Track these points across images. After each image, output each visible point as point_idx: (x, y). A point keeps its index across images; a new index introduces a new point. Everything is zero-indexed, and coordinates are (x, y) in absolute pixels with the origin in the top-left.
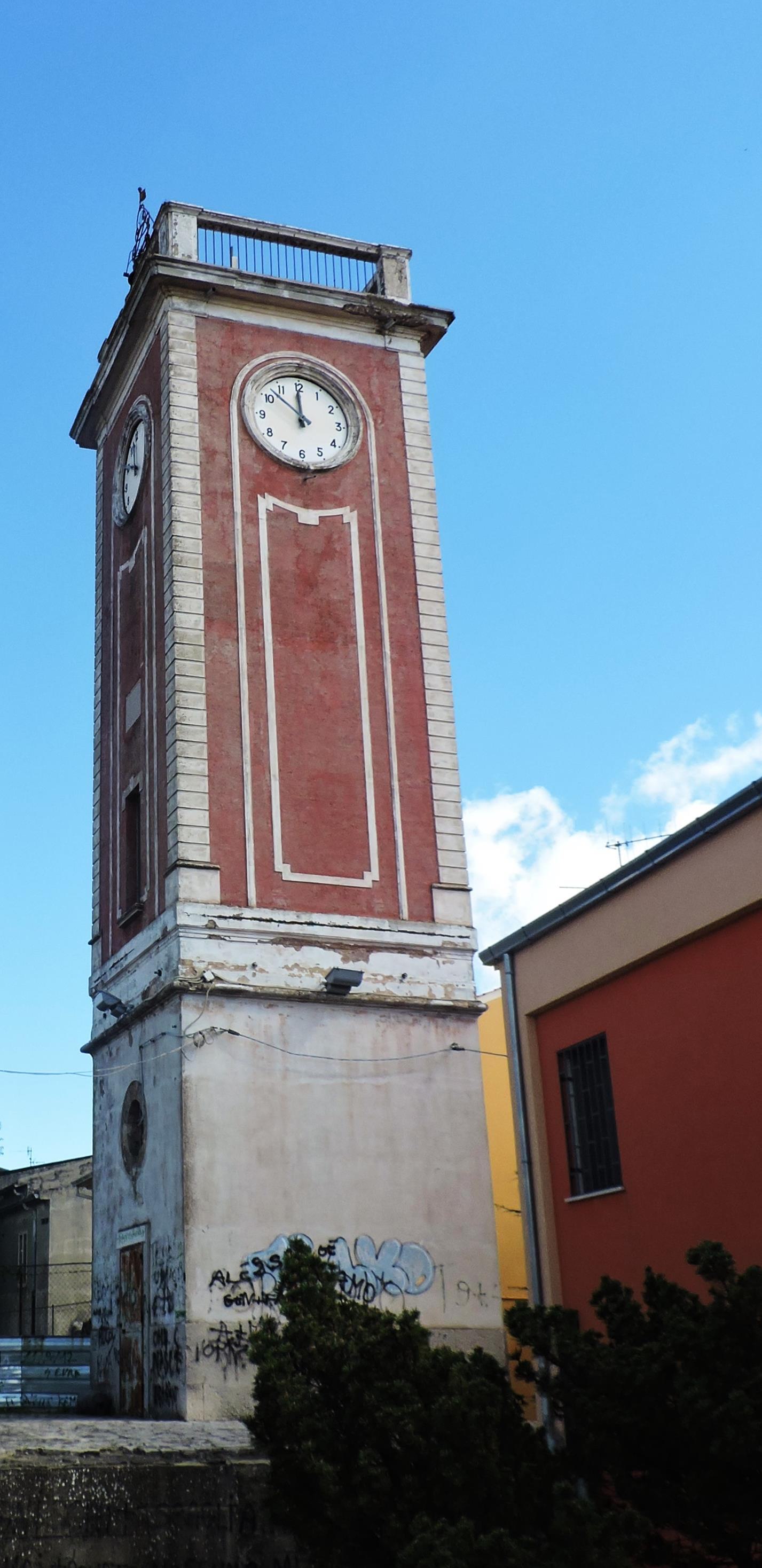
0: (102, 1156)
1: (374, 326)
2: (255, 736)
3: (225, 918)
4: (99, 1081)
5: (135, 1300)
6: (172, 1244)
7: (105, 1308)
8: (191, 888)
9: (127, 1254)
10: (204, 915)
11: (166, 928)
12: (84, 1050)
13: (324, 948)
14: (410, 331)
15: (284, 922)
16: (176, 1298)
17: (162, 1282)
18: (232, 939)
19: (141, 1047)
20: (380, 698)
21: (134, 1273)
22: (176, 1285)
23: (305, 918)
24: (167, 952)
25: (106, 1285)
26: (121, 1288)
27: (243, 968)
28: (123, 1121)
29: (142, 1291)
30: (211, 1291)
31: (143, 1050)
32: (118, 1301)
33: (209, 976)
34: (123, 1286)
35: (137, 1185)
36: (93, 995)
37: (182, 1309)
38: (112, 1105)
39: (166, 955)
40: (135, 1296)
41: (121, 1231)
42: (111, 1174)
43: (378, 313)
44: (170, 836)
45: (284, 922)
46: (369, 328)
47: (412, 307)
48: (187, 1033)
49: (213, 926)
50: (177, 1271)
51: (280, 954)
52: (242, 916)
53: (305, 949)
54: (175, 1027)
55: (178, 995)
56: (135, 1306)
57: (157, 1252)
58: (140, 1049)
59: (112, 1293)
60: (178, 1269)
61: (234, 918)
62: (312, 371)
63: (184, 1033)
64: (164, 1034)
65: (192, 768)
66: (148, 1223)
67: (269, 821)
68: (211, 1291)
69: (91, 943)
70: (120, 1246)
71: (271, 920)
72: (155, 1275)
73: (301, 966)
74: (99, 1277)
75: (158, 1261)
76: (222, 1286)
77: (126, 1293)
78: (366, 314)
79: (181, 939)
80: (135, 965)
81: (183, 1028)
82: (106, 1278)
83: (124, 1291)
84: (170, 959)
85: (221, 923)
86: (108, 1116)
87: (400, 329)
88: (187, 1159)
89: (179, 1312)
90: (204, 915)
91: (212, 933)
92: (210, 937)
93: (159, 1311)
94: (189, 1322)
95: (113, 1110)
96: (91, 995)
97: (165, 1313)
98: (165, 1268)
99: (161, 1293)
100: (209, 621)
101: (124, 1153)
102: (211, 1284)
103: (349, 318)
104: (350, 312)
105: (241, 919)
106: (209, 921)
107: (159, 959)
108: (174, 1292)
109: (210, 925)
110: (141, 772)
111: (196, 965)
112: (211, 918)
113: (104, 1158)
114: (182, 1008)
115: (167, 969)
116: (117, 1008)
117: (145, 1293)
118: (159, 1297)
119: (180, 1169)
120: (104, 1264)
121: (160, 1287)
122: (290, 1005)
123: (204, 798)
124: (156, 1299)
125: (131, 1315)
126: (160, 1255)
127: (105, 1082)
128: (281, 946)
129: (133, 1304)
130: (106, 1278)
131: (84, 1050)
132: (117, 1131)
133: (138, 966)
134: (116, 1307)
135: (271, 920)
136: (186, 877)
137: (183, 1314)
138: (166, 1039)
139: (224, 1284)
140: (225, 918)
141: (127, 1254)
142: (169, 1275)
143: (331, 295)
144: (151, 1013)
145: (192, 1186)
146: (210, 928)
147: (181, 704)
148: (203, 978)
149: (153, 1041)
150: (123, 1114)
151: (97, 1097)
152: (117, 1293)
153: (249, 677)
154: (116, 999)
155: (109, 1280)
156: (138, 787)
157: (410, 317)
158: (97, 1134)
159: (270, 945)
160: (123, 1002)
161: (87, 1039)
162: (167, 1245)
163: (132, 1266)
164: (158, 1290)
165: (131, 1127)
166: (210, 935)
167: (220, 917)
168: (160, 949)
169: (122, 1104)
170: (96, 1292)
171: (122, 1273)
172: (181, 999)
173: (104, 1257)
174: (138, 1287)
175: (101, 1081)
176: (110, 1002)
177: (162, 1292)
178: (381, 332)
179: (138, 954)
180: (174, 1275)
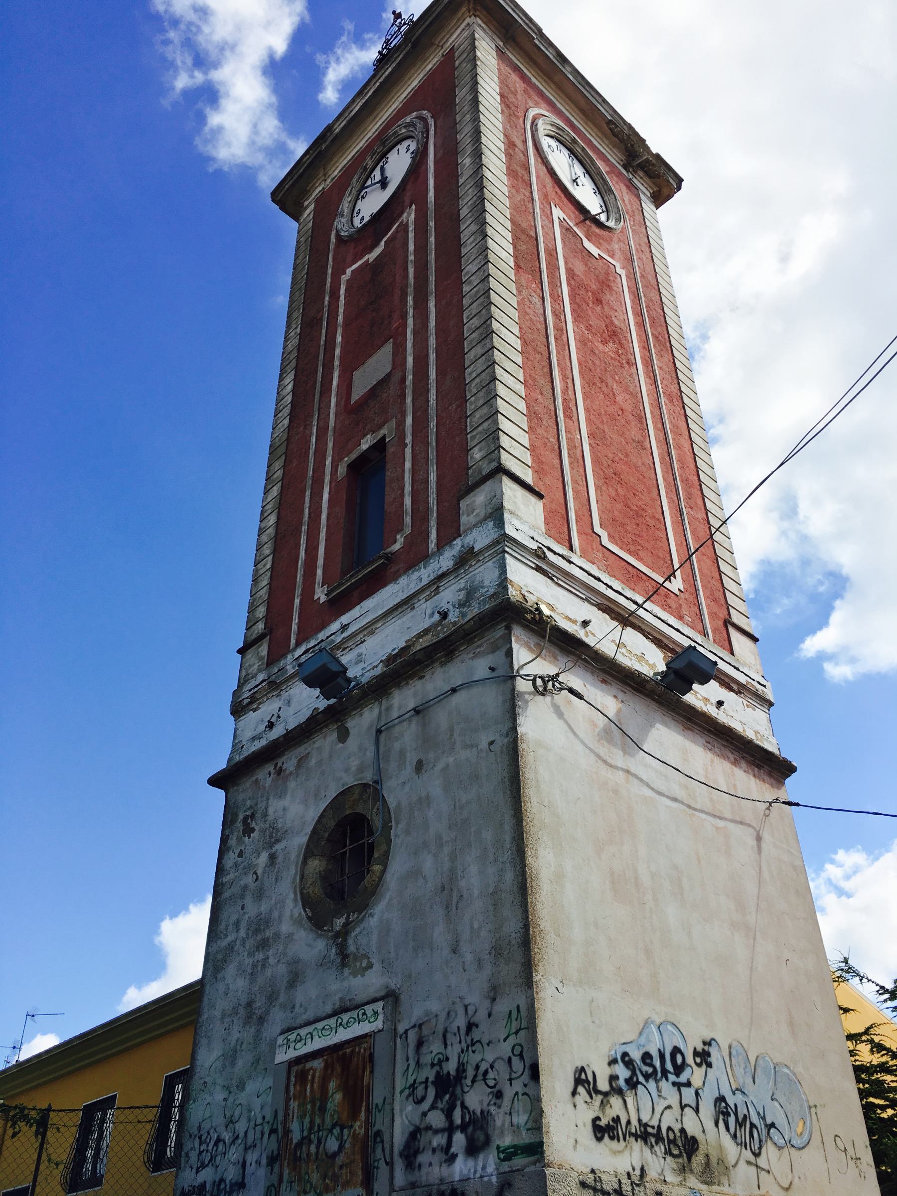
0: (237, 924)
1: (623, 158)
2: (565, 391)
3: (555, 553)
4: (241, 817)
5: (341, 1147)
6: (481, 1017)
7: (222, 1180)
8: (515, 502)
9: (317, 1064)
10: (533, 538)
11: (473, 548)
12: (215, 781)
13: (647, 638)
14: (647, 179)
15: (611, 587)
16: (500, 1119)
17: (439, 1096)
18: (560, 582)
19: (379, 731)
20: (660, 426)
21: (338, 1096)
22: (499, 1095)
23: (629, 594)
24: (463, 585)
25: (227, 1136)
26: (287, 1132)
27: (574, 622)
28: (309, 852)
29: (368, 1124)
30: (575, 1106)
31: (383, 735)
32: (272, 1160)
33: (546, 611)
34: (295, 1126)
35: (350, 941)
36: (238, 710)
37: (526, 1138)
38: (278, 841)
39: (460, 590)
40: (340, 1138)
41: (289, 1030)
42: (264, 945)
43: (632, 146)
44: (476, 449)
45: (611, 587)
46: (619, 158)
47: (658, 157)
48: (522, 672)
49: (543, 558)
50: (501, 1066)
51: (607, 624)
52: (572, 560)
53: (629, 630)
54: (492, 669)
55: (504, 624)
56: (339, 1160)
57: (420, 1044)
58: (377, 733)
59: (246, 1149)
60: (510, 1059)
61: (562, 556)
62: (583, 151)
63: (518, 671)
64: (454, 690)
65: (509, 381)
66: (391, 997)
67: (584, 479)
68: (575, 1106)
69: (241, 651)
70: (282, 1056)
71: (599, 580)
72: (413, 1087)
73: (628, 648)
74: (206, 1126)
75: (427, 1059)
76: (589, 1099)
77: (305, 1140)
78: (622, 141)
79: (507, 555)
80: (365, 632)
81: (516, 667)
82: (230, 1122)
83: (296, 1137)
84: (470, 593)
85: (550, 555)
86: (264, 857)
87: (641, 173)
88: (529, 860)
89: (514, 1146)
90: (533, 538)
91: (540, 565)
92: (538, 569)
93: (423, 1158)
94: (549, 1165)
95: (278, 847)
96: (231, 714)
97: (454, 1157)
98: (451, 1067)
99: (437, 1119)
100: (518, 267)
101: (306, 901)
102: (574, 1093)
103: (607, 138)
104: (610, 129)
105: (570, 562)
106: (538, 547)
107: (449, 595)
108: (492, 1109)
109: (540, 553)
110: (393, 423)
111: (527, 594)
112: (540, 546)
113: (243, 925)
114: (513, 639)
115: (461, 605)
116: (340, 680)
117: (379, 1124)
118: (429, 1128)
119: (509, 876)
120: (225, 1100)
121: (433, 1107)
122: (623, 689)
123: (523, 419)
124: (414, 1135)
125: (324, 1177)
126: (435, 1047)
127: (258, 815)
128: (608, 617)
129: (335, 1155)
130: (230, 1122)
131: (215, 781)
132: (291, 873)
133: (372, 633)
134: (262, 1172)
135: (599, 580)
136: (510, 488)
137: (536, 1149)
138: (456, 699)
139: (591, 1098)
140: (555, 553)
141: (317, 1064)
142: (468, 1082)
143: (603, 104)
144: (411, 677)
145: (539, 906)
146: (538, 557)
147: (497, 317)
148: (538, 609)
149: (417, 711)
150: (308, 846)
151: (232, 842)
152: (271, 1144)
153: (556, 339)
154: (342, 665)
155: (241, 1127)
156: (384, 437)
157: (653, 165)
158: (226, 894)
159: (595, 609)
160: (350, 674)
161: (222, 765)
162: (461, 1022)
163: (332, 1085)
164: (424, 1114)
165: (324, 863)
166: (537, 565)
167: (549, 549)
168: (442, 588)
169: (309, 829)
170: (193, 1155)
171: (294, 1104)
172: (509, 629)
173: (227, 1088)
174: (354, 1116)
175: (246, 819)
176: (335, 668)
177: (443, 1118)
178: (625, 167)
179: (380, 613)
180: (491, 1075)
